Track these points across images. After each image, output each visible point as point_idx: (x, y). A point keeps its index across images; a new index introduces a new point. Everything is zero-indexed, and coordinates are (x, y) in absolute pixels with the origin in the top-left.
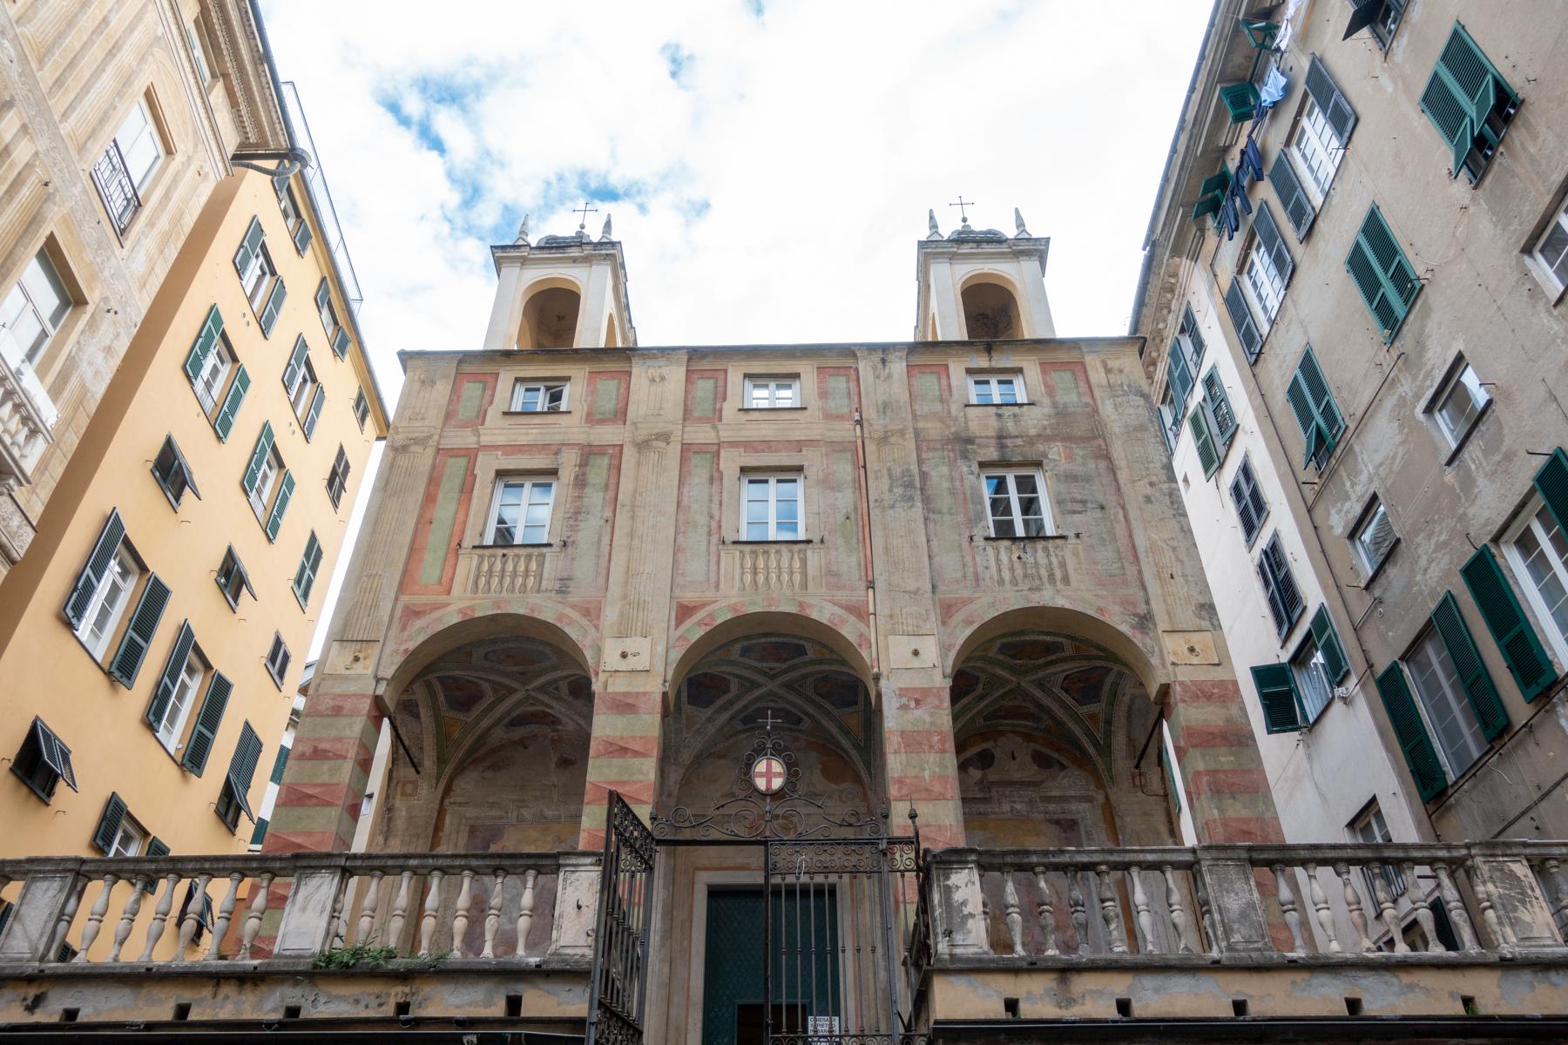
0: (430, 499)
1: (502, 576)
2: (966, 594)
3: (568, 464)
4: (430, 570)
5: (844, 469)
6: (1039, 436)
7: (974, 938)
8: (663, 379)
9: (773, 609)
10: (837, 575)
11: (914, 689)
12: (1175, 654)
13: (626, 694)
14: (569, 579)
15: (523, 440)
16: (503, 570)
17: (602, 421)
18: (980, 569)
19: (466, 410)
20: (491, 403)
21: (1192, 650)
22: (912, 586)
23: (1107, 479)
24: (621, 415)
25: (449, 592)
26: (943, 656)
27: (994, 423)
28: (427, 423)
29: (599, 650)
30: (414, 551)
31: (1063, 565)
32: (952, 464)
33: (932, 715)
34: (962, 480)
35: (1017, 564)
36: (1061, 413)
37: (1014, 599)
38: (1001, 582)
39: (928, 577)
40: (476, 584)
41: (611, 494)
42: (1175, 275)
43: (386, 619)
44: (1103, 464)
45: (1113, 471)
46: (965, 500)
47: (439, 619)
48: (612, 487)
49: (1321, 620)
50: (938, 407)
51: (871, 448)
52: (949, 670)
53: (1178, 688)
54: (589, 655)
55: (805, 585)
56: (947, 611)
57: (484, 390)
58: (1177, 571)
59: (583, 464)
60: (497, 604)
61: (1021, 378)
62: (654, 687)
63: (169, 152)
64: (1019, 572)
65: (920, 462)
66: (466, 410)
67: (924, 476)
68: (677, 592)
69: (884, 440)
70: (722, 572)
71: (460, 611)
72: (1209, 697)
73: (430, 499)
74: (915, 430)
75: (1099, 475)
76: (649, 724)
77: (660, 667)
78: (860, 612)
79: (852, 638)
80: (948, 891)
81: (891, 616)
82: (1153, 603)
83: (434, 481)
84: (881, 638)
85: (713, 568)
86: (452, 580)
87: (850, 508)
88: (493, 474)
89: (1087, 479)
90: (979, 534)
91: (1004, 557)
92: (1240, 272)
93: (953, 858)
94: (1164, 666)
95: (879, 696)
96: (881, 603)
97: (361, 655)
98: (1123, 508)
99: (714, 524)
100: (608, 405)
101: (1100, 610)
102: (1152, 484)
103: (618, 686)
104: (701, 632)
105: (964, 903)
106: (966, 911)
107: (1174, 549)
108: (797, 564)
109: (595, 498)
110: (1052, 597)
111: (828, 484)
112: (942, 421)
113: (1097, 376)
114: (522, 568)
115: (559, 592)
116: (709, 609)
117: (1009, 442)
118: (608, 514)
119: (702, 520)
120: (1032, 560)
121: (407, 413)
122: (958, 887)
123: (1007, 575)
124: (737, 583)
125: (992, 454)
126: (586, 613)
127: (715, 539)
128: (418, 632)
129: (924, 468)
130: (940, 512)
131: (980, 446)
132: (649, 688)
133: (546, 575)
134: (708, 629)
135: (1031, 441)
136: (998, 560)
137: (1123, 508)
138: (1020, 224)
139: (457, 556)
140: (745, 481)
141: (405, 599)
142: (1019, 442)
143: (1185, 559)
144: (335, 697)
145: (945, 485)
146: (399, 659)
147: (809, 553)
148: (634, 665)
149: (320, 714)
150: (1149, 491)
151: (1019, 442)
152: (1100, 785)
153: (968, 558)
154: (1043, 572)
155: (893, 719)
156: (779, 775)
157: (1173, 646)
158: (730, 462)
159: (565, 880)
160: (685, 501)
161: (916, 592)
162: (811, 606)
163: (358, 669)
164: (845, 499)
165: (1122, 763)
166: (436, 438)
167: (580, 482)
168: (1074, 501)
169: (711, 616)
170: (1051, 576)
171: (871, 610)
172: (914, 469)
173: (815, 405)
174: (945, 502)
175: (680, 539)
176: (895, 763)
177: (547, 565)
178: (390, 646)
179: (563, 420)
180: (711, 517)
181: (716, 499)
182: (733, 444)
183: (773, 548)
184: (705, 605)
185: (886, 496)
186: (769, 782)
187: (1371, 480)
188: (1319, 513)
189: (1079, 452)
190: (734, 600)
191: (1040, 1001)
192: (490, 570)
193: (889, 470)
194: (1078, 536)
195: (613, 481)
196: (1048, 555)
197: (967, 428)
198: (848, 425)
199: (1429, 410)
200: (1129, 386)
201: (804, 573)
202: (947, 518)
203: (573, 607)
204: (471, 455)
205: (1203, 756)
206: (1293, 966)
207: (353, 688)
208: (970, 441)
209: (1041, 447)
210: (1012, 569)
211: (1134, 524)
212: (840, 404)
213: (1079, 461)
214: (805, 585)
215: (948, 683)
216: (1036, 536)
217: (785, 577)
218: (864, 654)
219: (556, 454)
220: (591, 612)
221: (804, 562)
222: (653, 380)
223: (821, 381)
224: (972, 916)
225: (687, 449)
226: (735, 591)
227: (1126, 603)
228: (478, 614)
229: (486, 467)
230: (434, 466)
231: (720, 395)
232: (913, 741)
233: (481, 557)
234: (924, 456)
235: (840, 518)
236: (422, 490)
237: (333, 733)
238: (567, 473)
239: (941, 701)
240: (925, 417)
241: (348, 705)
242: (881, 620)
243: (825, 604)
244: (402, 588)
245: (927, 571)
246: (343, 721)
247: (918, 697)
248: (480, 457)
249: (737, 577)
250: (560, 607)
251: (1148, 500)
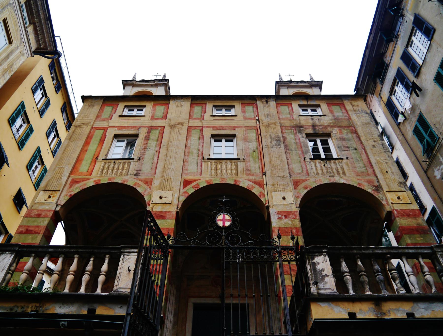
0: (87, 143)
1: (113, 169)
2: (304, 178)
4: (84, 167)
5: (252, 135)
6: (328, 126)
7: (329, 285)
8: (181, 105)
9: (224, 182)
10: (250, 171)
11: (284, 212)
12: (392, 200)
13: (161, 212)
14: (140, 171)
16: (114, 167)
17: (157, 119)
18: (309, 170)
20: (115, 113)
21: (399, 198)
22: (281, 174)
23: (357, 140)
24: (165, 117)
25: (91, 175)
26: (296, 200)
28: (89, 118)
30: (79, 160)
31: (342, 168)
32: (295, 134)
33: (292, 221)
34: (299, 140)
35: (324, 168)
37: (324, 180)
38: (318, 174)
39: (288, 171)
40: (102, 172)
41: (159, 142)
43: (64, 183)
44: (354, 135)
45: (359, 137)
46: (301, 146)
47: (85, 184)
48: (160, 140)
50: (288, 116)
51: (263, 129)
52: (298, 205)
53: (395, 212)
54: (146, 198)
55: (237, 174)
56: (296, 184)
57: (113, 109)
58: (389, 170)
59: (149, 132)
60: (110, 179)
61: (319, 108)
62: (173, 210)
63: (10, 42)
64: (325, 170)
65: (282, 133)
67: (284, 138)
68: (184, 176)
70: (203, 169)
71: (95, 181)
73: (87, 143)
74: (280, 123)
75: (354, 138)
77: (176, 202)
79: (257, 193)
80: (314, 265)
81: (273, 185)
82: (381, 182)
83: (89, 137)
84: (269, 193)
85: (199, 167)
86: (93, 170)
87: (255, 148)
88: (113, 135)
89: (349, 140)
91: (318, 165)
92: (391, 94)
94: (388, 204)
95: (269, 214)
96: (268, 180)
97: (52, 196)
98: (364, 149)
99: (200, 153)
101: (359, 184)
102: (375, 141)
103: (158, 209)
104: (193, 190)
105: (323, 270)
106: (324, 273)
107: (387, 163)
108: (234, 167)
110: (338, 179)
111: (246, 140)
112: (290, 120)
114: (121, 167)
115: (135, 175)
116: (197, 182)
117: (317, 127)
118: (157, 149)
119: (195, 151)
120: (329, 166)
121: (82, 115)
122: (319, 263)
123: (320, 172)
124: (209, 173)
125: (311, 131)
126: (146, 183)
127: (200, 158)
128: (76, 189)
129: (284, 135)
130: (291, 150)
131: (306, 129)
132: (171, 210)
133: (131, 169)
134: (197, 189)
135: (326, 127)
136: (316, 166)
137: (364, 149)
139: (96, 162)
140: (213, 140)
141: (72, 177)
142: (321, 127)
143: (391, 166)
144: (38, 210)
145: (293, 141)
146: (67, 198)
147: (239, 163)
149: (31, 217)
150: (374, 143)
151: (321, 127)
153: (304, 166)
154: (335, 171)
155: (275, 222)
156: (229, 220)
157: (391, 197)
158: (207, 133)
159: (123, 259)
160: (188, 145)
161: (283, 177)
162: (240, 181)
163: (50, 200)
164: (253, 145)
166: (92, 123)
167: (147, 138)
168: (344, 147)
169: (198, 185)
170: (338, 173)
171: (265, 183)
172: (280, 135)
174: (293, 147)
175: (186, 157)
177: (131, 166)
178: (64, 193)
180: (199, 150)
181: (201, 144)
182: (208, 127)
183: (224, 162)
184: (195, 181)
185: (270, 144)
186: (224, 223)
188: (429, 173)
189: (344, 131)
190: (207, 179)
192: (108, 167)
193: (270, 135)
194: (347, 158)
195: (160, 138)
196: (336, 165)
197: (300, 123)
200: (361, 110)
201: (237, 170)
202: (294, 152)
203: (141, 180)
204: (105, 129)
205: (410, 238)
207: (46, 207)
208: (302, 127)
209: (330, 129)
210: (322, 170)
211: (369, 154)
213: (345, 134)
215: (298, 210)
216: (329, 158)
217: (229, 171)
218: (263, 199)
219: (138, 129)
220: (148, 182)
221: (237, 166)
222: (178, 106)
224: (327, 276)
226: (208, 176)
227: (369, 182)
228: (102, 182)
229: (110, 133)
230: (90, 132)
231: (204, 111)
233: (105, 163)
234: (284, 131)
235: (251, 151)
236: (84, 140)
237: (36, 224)
238: (142, 136)
239: (296, 216)
240: (283, 119)
241: (43, 214)
242: (269, 186)
243: (245, 181)
244: (71, 173)
245: (287, 169)
246: (41, 219)
249: (209, 171)
250: (136, 181)
251: (374, 146)
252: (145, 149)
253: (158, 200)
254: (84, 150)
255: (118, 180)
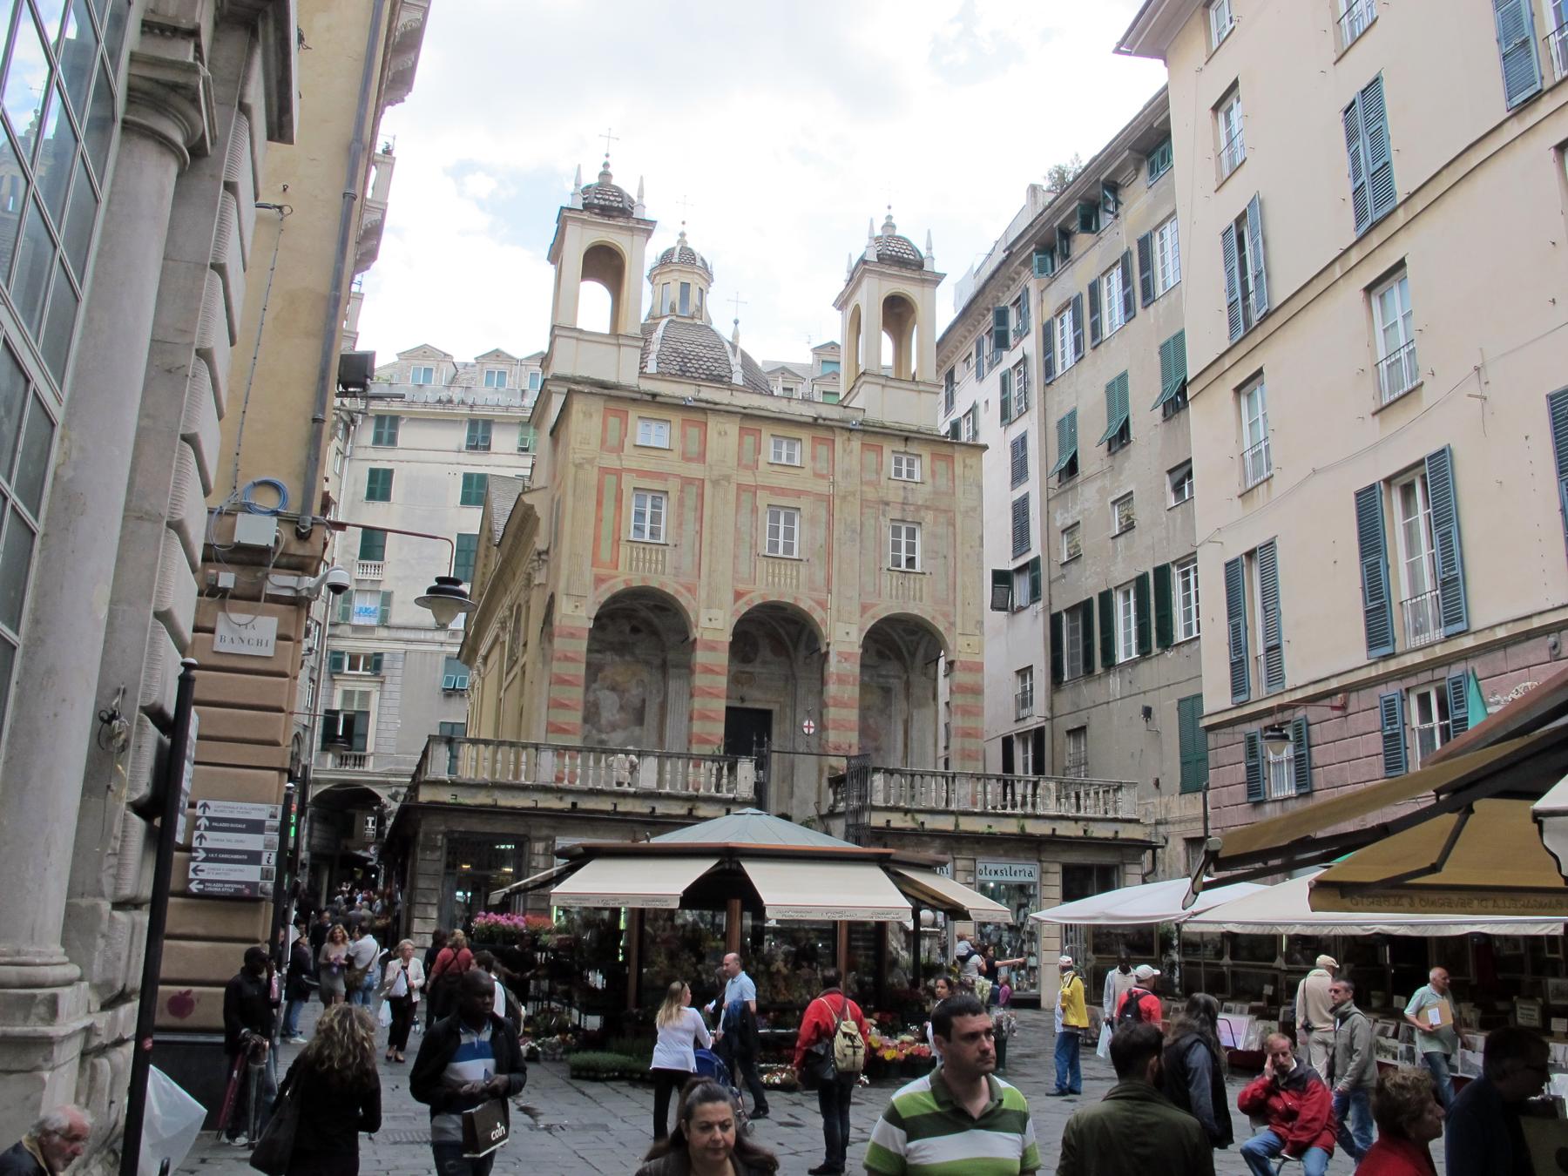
0: (599, 503)
3: (673, 486)
4: (605, 555)
5: (822, 514)
15: (647, 467)
19: (613, 439)
24: (702, 457)
27: (901, 493)
29: (697, 616)
30: (597, 539)
36: (936, 493)
37: (895, 608)
42: (1019, 274)
49: (1036, 561)
50: (874, 477)
51: (837, 502)
55: (798, 586)
56: (864, 608)
62: (727, 638)
66: (613, 439)
69: (844, 498)
72: (971, 670)
76: (723, 658)
78: (823, 605)
83: (600, 491)
90: (885, 567)
93: (876, 770)
96: (832, 602)
100: (694, 448)
103: (708, 636)
104: (745, 609)
109: (690, 516)
110: (914, 609)
111: (813, 521)
113: (958, 469)
125: (898, 516)
126: (689, 590)
135: (918, 508)
138: (929, 248)
148: (713, 624)
152: (906, 671)
155: (833, 665)
164: (821, 533)
165: (919, 661)
173: (808, 464)
176: (832, 689)
179: (668, 454)
182: (764, 488)
187: (1080, 513)
188: (1052, 504)
189: (942, 519)
191: (898, 821)
198: (825, 482)
199: (1114, 503)
204: (618, 473)
206: (975, 814)
207: (578, 624)
208: (887, 504)
212: (822, 466)
214: (798, 586)
220: (691, 589)
223: (814, 448)
225: (739, 486)
227: (945, 615)
229: (629, 482)
232: (841, 680)
238: (674, 495)
247: (845, 657)
248: (624, 475)
252: (680, 525)
253: (707, 624)
254: (599, 520)
255: (654, 584)
